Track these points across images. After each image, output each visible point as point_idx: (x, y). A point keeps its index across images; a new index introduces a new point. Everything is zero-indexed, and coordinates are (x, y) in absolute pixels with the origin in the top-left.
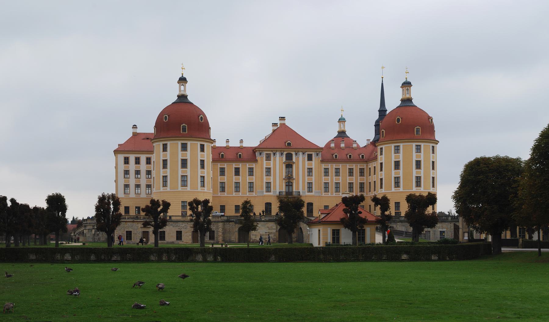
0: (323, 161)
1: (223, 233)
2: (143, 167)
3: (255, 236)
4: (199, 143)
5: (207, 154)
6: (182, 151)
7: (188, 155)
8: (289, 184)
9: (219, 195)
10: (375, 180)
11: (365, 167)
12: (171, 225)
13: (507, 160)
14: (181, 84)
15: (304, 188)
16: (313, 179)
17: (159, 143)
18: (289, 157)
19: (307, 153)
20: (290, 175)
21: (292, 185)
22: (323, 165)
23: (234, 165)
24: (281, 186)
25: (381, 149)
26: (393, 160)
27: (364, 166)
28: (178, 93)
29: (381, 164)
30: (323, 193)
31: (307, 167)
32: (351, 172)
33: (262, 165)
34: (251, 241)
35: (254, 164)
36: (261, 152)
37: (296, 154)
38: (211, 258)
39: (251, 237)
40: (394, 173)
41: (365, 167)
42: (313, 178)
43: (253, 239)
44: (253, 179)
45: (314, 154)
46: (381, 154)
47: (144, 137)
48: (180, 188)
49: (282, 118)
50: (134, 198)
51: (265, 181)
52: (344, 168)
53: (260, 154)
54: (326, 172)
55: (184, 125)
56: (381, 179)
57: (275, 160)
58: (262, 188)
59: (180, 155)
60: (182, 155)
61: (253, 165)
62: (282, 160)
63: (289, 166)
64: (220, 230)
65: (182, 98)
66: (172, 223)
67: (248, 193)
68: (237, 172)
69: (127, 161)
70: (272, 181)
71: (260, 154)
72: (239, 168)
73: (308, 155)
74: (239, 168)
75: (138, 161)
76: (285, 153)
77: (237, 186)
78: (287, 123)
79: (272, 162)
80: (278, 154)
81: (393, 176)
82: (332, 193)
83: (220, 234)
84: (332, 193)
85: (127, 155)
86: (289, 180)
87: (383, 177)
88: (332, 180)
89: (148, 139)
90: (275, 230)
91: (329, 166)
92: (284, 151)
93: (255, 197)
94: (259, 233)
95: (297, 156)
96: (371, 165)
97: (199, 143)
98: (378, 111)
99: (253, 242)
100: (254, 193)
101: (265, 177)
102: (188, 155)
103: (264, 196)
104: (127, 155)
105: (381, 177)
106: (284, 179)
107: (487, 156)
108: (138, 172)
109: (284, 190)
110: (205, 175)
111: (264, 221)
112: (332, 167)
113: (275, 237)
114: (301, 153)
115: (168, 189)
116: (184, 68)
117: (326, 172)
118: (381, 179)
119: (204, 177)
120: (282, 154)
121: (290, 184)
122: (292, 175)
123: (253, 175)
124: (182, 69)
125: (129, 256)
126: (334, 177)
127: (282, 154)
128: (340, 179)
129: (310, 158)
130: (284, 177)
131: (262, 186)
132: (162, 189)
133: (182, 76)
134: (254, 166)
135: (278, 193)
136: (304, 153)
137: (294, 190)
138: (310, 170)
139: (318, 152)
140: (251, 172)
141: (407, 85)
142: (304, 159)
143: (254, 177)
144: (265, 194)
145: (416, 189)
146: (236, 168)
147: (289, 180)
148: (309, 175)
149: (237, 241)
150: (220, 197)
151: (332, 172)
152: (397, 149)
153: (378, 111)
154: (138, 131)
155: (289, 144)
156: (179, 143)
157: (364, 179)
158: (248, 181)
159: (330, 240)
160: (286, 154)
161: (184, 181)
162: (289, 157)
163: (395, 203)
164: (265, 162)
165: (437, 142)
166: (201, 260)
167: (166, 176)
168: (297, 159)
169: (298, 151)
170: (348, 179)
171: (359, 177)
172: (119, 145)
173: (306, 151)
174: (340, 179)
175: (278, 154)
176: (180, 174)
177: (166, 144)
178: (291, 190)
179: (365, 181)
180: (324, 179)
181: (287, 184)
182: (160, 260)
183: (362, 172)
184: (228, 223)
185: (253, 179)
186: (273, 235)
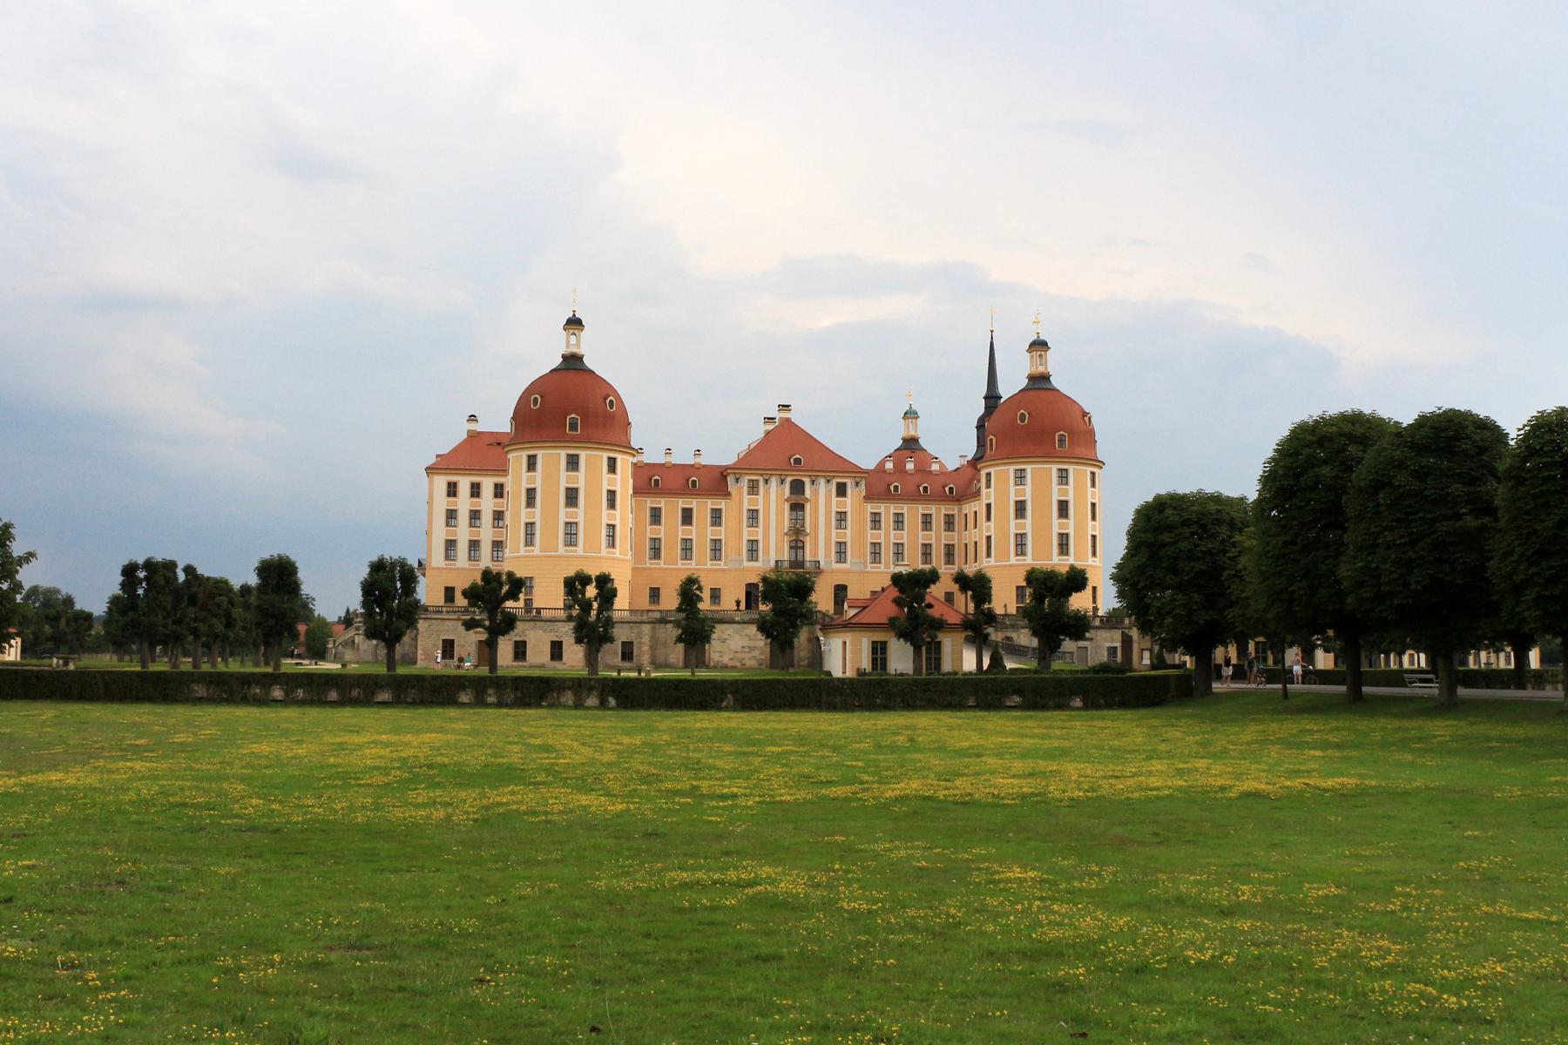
0: (870, 497)
1: (653, 648)
2: (487, 503)
3: (718, 654)
4: (605, 455)
5: (622, 479)
6: (568, 470)
7: (580, 480)
8: (797, 545)
9: (648, 565)
10: (977, 539)
11: (956, 512)
12: (541, 628)
13: (1217, 499)
14: (571, 331)
15: (827, 555)
16: (848, 535)
18: (797, 487)
19: (834, 481)
20: (798, 526)
21: (803, 548)
22: (869, 506)
23: (682, 503)
24: (779, 550)
25: (989, 475)
26: (1013, 498)
27: (953, 509)
28: (563, 350)
29: (989, 506)
30: (869, 565)
31: (835, 509)
32: (927, 521)
33: (741, 502)
34: (712, 664)
35: (723, 502)
36: (738, 476)
37: (813, 482)
38: (592, 701)
41: (956, 512)
42: (848, 532)
44: (721, 532)
45: (849, 483)
46: (988, 486)
48: (562, 550)
49: (785, 407)
51: (745, 537)
52: (913, 512)
53: (737, 480)
54: (876, 521)
55: (573, 415)
56: (989, 538)
57: (767, 493)
58: (740, 554)
59: (564, 479)
60: (568, 479)
61: (721, 504)
62: (784, 494)
63: (797, 507)
64: (646, 639)
65: (573, 362)
66: (542, 623)
67: (648, 561)
68: (687, 517)
69: (452, 490)
70: (760, 538)
71: (737, 480)
72: (690, 510)
73: (838, 484)
74: (690, 510)
75: (476, 490)
76: (789, 479)
77: (687, 548)
78: (795, 416)
79: (760, 498)
80: (774, 481)
81: (1013, 531)
82: (887, 566)
83: (646, 648)
85: (453, 478)
87: (992, 533)
88: (887, 536)
89: (499, 444)
91: (881, 508)
93: (724, 570)
95: (814, 487)
96: (969, 508)
97: (605, 455)
99: (715, 667)
100: (722, 563)
101: (746, 530)
102: (580, 480)
103: (745, 570)
104: (453, 478)
105: (989, 534)
107: (1181, 491)
108: (475, 515)
109: (786, 557)
110: (617, 522)
111: (738, 623)
112: (887, 510)
113: (763, 657)
114: (822, 481)
115: (536, 550)
117: (876, 521)
118: (989, 538)
119: (614, 526)
120: (782, 482)
121: (800, 544)
122: (803, 526)
123: (720, 525)
125: (413, 694)
126: (892, 533)
127: (782, 482)
128: (904, 537)
129: (841, 490)
130: (786, 530)
131: (740, 549)
132: (523, 550)
133: (574, 315)
134: (723, 506)
135: (772, 564)
136: (828, 481)
137: (808, 558)
138: (842, 517)
139: (858, 480)
140: (717, 517)
143: (722, 529)
144: (747, 564)
146: (684, 510)
148: (839, 527)
149: (681, 664)
150: (650, 569)
151: (887, 520)
154: (479, 427)
155: (798, 461)
156: (563, 454)
157: (954, 538)
158: (710, 537)
159: (866, 664)
160: (792, 482)
161: (571, 534)
162: (797, 487)
164: (746, 497)
166: (571, 702)
168: (815, 493)
170: (922, 537)
171: (943, 533)
172: (438, 456)
173: (834, 477)
174: (904, 537)
175: (774, 481)
176: (562, 519)
177: (534, 456)
178: (800, 558)
179: (955, 542)
180: (871, 536)
181: (794, 545)
182: (480, 702)
183: (949, 523)
184: (662, 625)
185: (721, 532)
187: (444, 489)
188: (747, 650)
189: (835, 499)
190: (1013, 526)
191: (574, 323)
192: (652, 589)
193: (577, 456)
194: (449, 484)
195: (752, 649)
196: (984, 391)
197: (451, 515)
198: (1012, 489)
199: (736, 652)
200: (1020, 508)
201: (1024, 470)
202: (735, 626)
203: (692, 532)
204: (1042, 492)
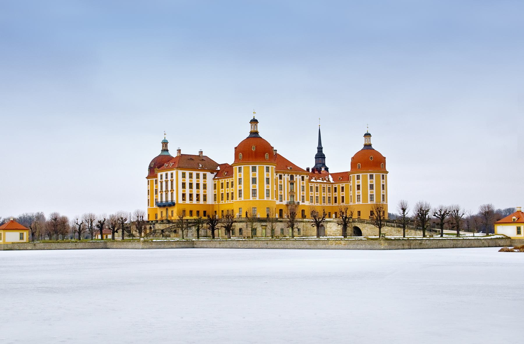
3: (329, 232)
17: (236, 167)
18: (292, 177)
19: (301, 176)
31: (301, 185)
39: (327, 233)
41: (331, 186)
43: (329, 234)
47: (189, 158)
50: (196, 204)
60: (253, 175)
69: (184, 176)
76: (290, 175)
84: (314, 204)
86: (292, 194)
90: (340, 228)
92: (290, 173)
94: (332, 230)
98: (317, 148)
106: (289, 193)
108: (191, 185)
116: (255, 113)
120: (288, 175)
124: (254, 113)
127: (288, 175)
133: (254, 118)
141: (368, 135)
145: (358, 203)
147: (292, 194)
151: (314, 189)
152: (254, 169)
153: (317, 148)
162: (292, 177)
163: (358, 211)
165: (387, 172)
167: (241, 190)
186: (339, 231)
188: (337, 231)
189: (301, 182)
195: (338, 230)
196: (317, 145)
197: (184, 185)
199: (334, 231)
200: (358, 186)
202: (334, 223)
204: (378, 183)
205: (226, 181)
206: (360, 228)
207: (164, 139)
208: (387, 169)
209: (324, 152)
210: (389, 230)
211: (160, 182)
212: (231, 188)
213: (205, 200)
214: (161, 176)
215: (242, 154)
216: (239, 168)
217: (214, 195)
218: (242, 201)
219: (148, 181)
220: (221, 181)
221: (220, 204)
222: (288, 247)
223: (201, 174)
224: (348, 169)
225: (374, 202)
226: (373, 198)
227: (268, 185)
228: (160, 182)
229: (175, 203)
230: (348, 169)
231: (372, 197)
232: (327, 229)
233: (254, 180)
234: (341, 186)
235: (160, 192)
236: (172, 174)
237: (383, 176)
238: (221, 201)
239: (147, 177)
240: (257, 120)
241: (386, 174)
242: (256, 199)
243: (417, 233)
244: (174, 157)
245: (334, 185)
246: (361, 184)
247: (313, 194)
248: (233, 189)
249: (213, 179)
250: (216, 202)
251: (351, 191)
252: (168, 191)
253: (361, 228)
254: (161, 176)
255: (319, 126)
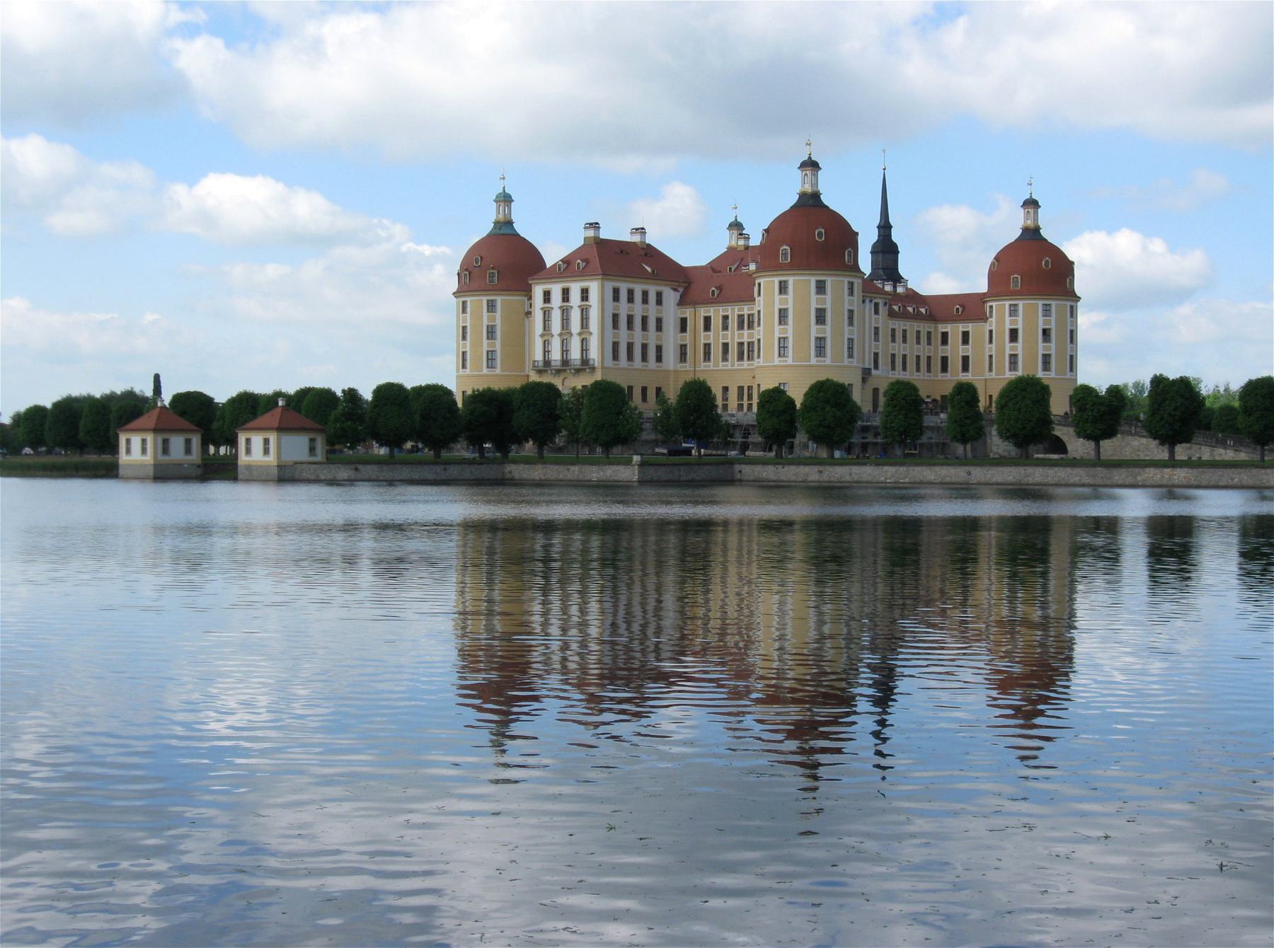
11: (932, 330)
15: (870, 364)
19: (873, 302)
26: (1041, 326)
40: (1041, 348)
88: (899, 348)
97: (846, 280)
112: (899, 325)
133: (810, 158)
136: (871, 301)
142: (870, 309)
154: (604, 235)
169: (867, 297)
173: (875, 298)
187: (609, 295)
190: (1008, 348)
191: (811, 165)
192: (657, 388)
193: (824, 281)
194: (563, 290)
196: (877, 220)
198: (1041, 319)
201: (1049, 305)
203: (687, 338)
204: (1061, 323)
205: (721, 313)
206: (1061, 437)
207: (501, 191)
208: (1078, 288)
209: (895, 237)
210: (1143, 444)
211: (542, 309)
212: (736, 333)
213: (659, 358)
214: (547, 296)
215: (791, 249)
216: (780, 282)
217: (679, 347)
218: (828, 366)
219: (464, 303)
220: (703, 312)
221: (698, 371)
222: (1028, 480)
223: (652, 291)
224: (982, 286)
225: (1020, 373)
226: (1049, 363)
227: (851, 328)
228: (542, 309)
229: (596, 365)
230: (982, 286)
231: (1048, 361)
232: (991, 439)
233: (821, 317)
234: (961, 329)
235: (542, 336)
236: (585, 294)
237: (1072, 307)
238: (703, 364)
239: (455, 290)
240: (818, 162)
241: (1073, 304)
242: (825, 361)
243: (1216, 452)
244: (986, 291)
245: (940, 326)
246: (1020, 326)
247: (902, 347)
248: (879, 345)
249: (678, 305)
250: (687, 365)
251: (991, 342)
252: (571, 335)
253: (1065, 438)
254: (547, 296)
255: (884, 169)
